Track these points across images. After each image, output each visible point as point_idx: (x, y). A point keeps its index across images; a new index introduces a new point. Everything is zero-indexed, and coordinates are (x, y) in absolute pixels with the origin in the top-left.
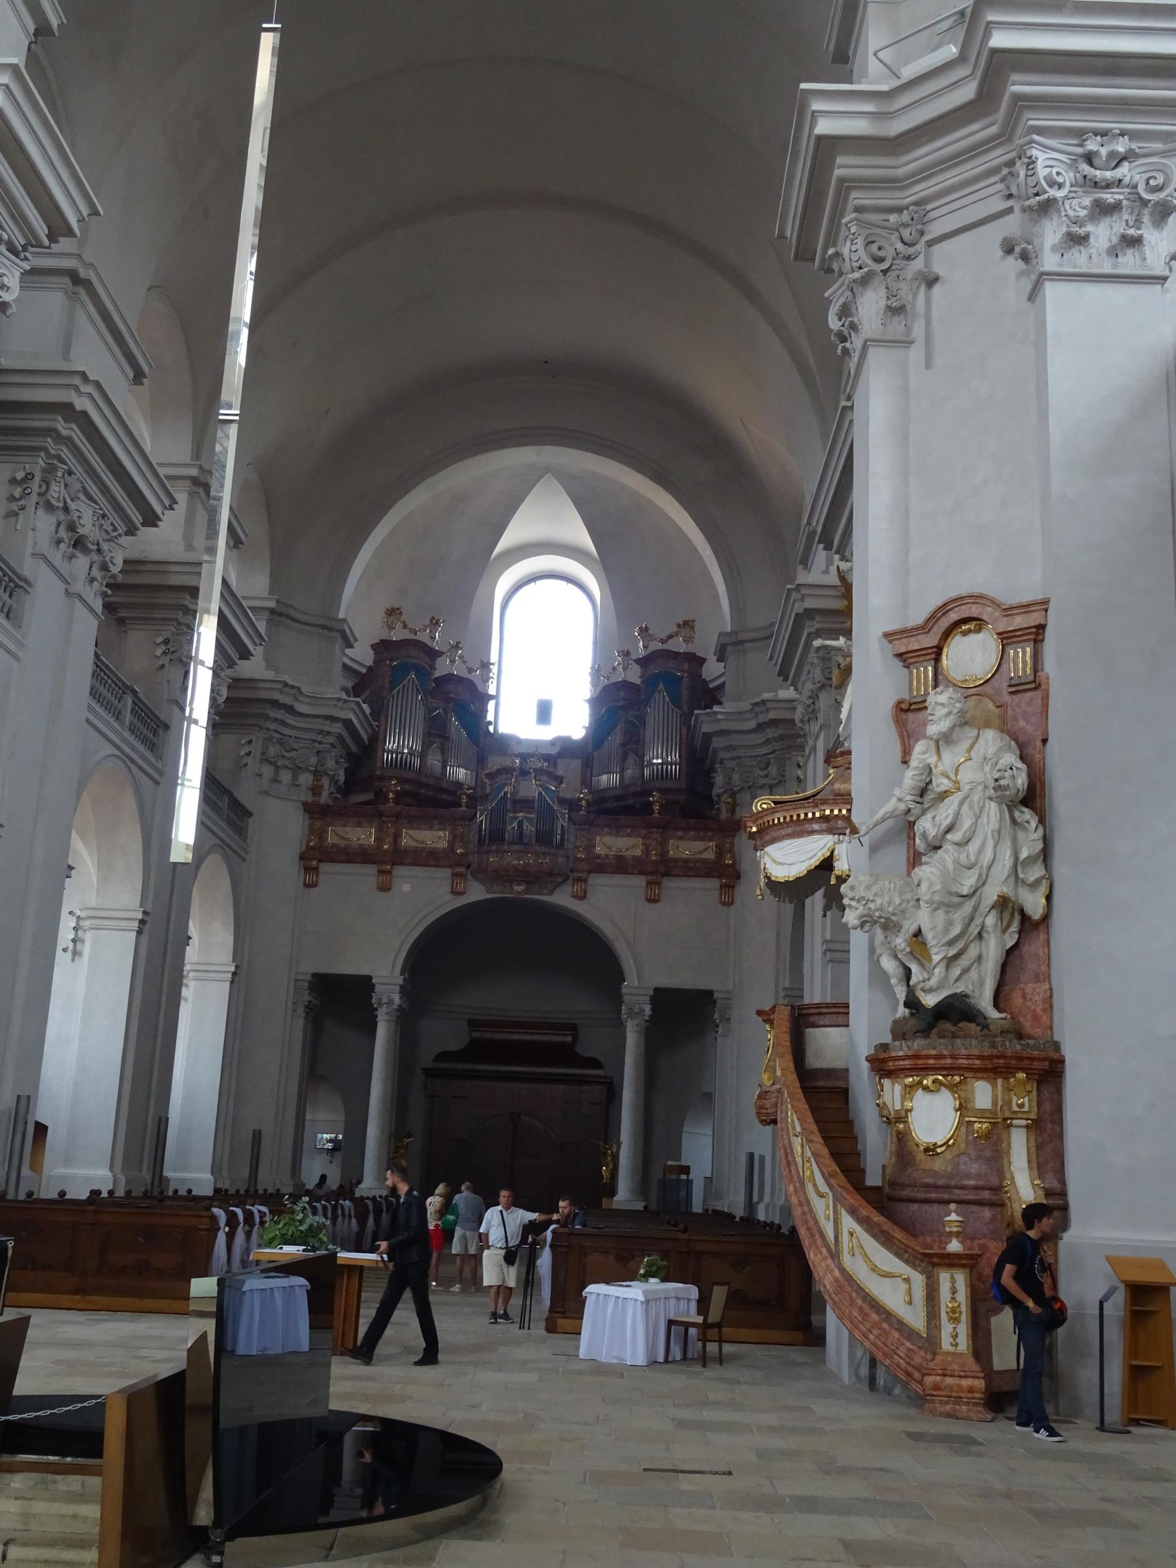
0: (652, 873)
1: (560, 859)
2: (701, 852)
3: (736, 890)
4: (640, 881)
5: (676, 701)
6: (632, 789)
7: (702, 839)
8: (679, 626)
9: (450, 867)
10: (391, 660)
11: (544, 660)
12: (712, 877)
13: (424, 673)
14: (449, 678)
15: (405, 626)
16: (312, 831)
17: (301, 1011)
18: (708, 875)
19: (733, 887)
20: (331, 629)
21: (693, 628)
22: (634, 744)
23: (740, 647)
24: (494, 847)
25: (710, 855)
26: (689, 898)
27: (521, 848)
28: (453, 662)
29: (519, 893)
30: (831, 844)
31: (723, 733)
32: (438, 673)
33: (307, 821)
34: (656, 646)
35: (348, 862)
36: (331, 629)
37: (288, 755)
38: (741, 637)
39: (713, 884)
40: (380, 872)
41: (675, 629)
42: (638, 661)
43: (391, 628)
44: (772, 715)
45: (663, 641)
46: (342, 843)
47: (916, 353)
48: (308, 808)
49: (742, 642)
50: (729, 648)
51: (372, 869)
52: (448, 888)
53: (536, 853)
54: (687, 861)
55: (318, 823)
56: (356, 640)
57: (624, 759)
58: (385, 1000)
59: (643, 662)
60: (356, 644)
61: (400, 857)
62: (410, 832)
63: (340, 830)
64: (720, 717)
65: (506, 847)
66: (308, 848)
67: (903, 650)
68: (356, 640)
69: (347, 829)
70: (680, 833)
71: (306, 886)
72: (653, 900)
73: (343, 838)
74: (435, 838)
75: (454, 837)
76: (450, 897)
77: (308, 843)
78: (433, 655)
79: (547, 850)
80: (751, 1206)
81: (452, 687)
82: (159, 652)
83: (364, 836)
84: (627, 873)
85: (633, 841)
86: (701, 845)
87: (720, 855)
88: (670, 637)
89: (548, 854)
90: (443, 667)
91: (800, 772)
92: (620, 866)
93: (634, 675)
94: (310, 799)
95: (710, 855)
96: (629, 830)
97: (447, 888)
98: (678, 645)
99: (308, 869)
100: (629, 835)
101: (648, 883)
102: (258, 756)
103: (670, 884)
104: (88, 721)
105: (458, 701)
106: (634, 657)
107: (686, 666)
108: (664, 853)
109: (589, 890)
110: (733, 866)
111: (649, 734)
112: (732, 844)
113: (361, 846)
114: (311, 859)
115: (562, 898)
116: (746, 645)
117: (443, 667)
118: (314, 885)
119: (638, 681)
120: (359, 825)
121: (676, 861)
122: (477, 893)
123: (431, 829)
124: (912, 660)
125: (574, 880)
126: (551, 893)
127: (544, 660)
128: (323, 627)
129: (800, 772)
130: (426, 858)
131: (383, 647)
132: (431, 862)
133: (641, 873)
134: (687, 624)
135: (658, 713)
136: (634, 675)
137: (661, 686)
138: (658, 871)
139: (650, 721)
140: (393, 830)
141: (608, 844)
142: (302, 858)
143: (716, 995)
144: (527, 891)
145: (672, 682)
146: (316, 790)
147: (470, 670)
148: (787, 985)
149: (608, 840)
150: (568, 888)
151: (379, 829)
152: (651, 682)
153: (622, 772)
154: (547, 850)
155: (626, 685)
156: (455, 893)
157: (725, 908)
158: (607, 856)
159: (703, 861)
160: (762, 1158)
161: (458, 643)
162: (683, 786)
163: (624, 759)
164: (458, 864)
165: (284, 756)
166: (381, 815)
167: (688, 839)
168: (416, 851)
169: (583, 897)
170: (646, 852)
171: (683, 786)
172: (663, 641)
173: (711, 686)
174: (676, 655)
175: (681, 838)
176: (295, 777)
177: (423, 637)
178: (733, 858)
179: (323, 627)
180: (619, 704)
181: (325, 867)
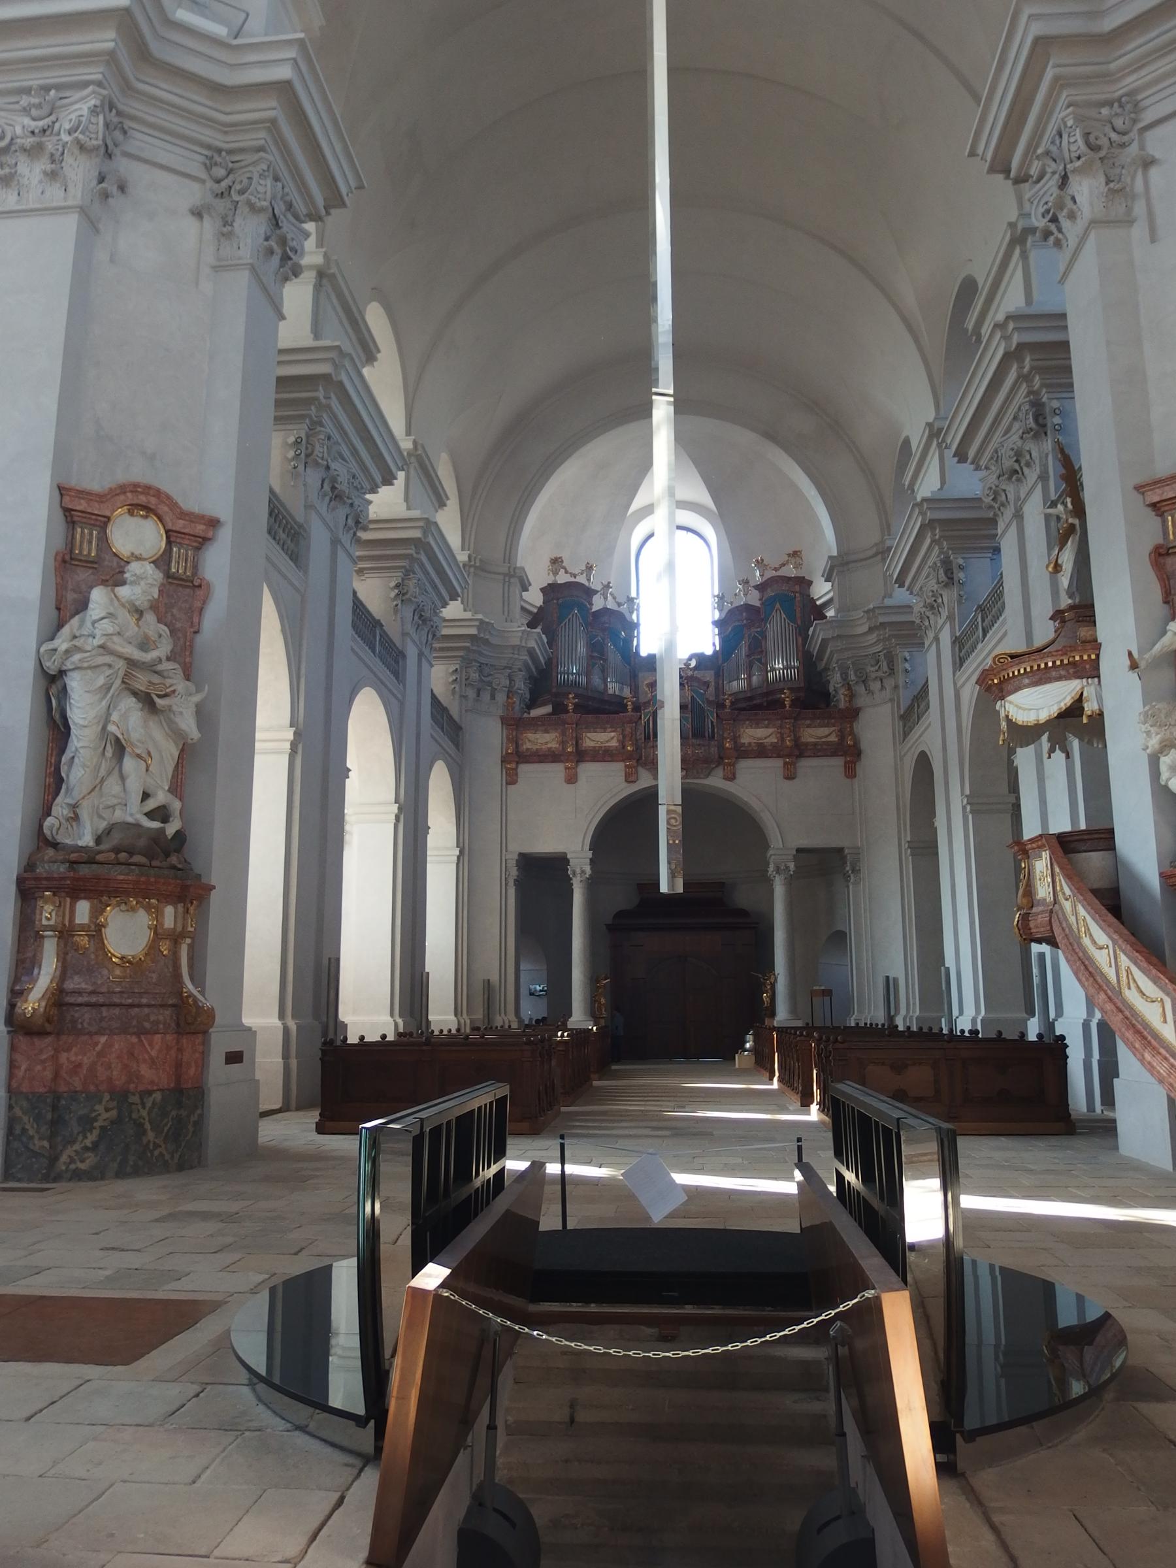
0: (788, 756)
4: (777, 764)
5: (791, 617)
6: (759, 691)
7: (827, 726)
8: (789, 555)
11: (676, 596)
13: (584, 608)
14: (605, 611)
15: (566, 572)
17: (511, 883)
18: (834, 754)
22: (758, 653)
25: (833, 738)
26: (818, 774)
28: (606, 598)
30: (1079, 687)
32: (594, 609)
34: (770, 574)
39: (838, 762)
40: (567, 768)
42: (757, 587)
43: (556, 573)
44: (882, 619)
45: (776, 569)
47: (1138, 232)
48: (504, 721)
49: (847, 563)
54: (815, 744)
57: (750, 666)
58: (578, 871)
59: (761, 588)
61: (581, 755)
63: (530, 736)
66: (507, 753)
67: (1156, 499)
69: (537, 736)
70: (808, 722)
75: (624, 737)
76: (626, 784)
78: (589, 593)
80: (891, 1018)
81: (605, 619)
82: (393, 594)
83: (546, 740)
85: (770, 731)
87: (842, 738)
88: (783, 565)
90: (598, 603)
91: (907, 666)
92: (761, 752)
95: (833, 738)
98: (790, 571)
100: (767, 727)
101: (785, 764)
102: (464, 682)
104: (352, 649)
105: (611, 628)
106: (752, 583)
107: (797, 588)
108: (796, 740)
111: (770, 645)
112: (852, 727)
116: (851, 566)
117: (598, 603)
118: (514, 782)
119: (758, 604)
120: (547, 731)
121: (807, 744)
124: (1167, 508)
126: (707, 776)
127: (676, 596)
129: (907, 666)
130: (603, 755)
131: (550, 591)
133: (779, 756)
134: (796, 554)
135: (777, 628)
136: (754, 599)
137: (778, 606)
138: (793, 754)
139: (770, 635)
141: (752, 734)
143: (846, 851)
145: (786, 602)
146: (509, 706)
147: (619, 605)
148: (909, 839)
150: (719, 772)
151: (563, 734)
152: (768, 603)
153: (750, 677)
155: (747, 607)
157: (849, 780)
158: (750, 744)
159: (828, 743)
160: (896, 980)
162: (802, 685)
163: (750, 666)
166: (564, 723)
169: (731, 777)
170: (782, 739)
171: (802, 685)
172: (776, 569)
173: (818, 603)
175: (809, 726)
177: (582, 579)
180: (741, 625)
181: (523, 768)
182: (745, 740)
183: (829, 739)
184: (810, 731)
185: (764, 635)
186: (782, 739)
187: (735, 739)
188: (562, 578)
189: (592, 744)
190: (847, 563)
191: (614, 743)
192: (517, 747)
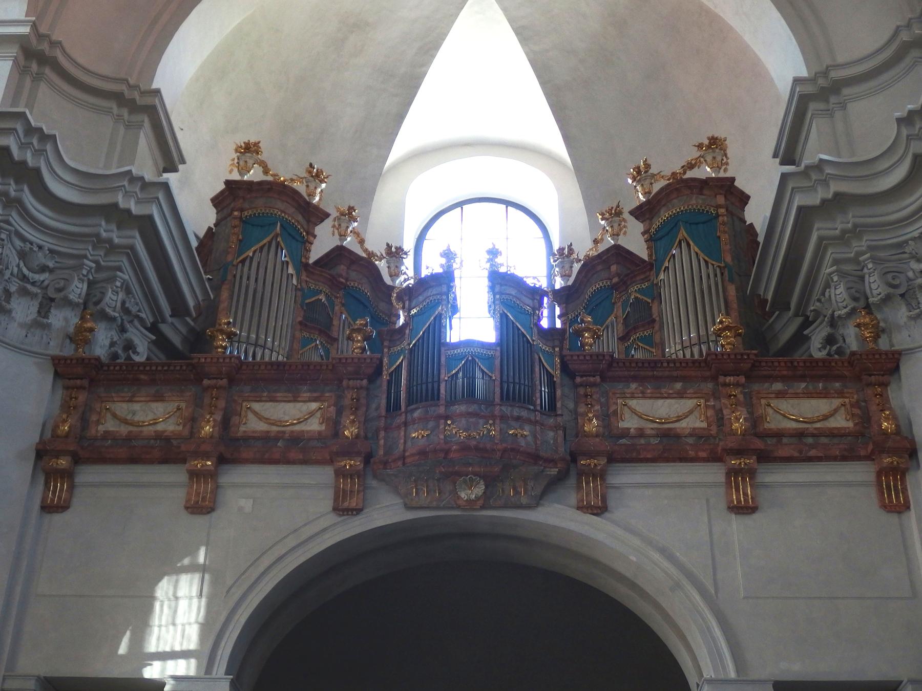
0: (739, 452)
1: (551, 434)
2: (826, 418)
3: (909, 479)
4: (714, 474)
8: (700, 146)
9: (331, 462)
10: (242, 210)
12: (859, 458)
15: (266, 172)
16: (66, 407)
18: (848, 456)
19: (903, 474)
20: (133, 107)
21: (724, 150)
23: (833, 99)
24: (416, 414)
27: (473, 408)
29: (470, 504)
31: (840, 202)
33: (60, 393)
35: (133, 460)
36: (133, 107)
37: (37, 277)
38: (835, 74)
39: (861, 473)
41: (696, 153)
43: (243, 170)
46: (124, 430)
48: (63, 370)
49: (836, 87)
50: (813, 106)
51: (175, 475)
52: (329, 504)
53: (503, 418)
54: (800, 435)
55: (82, 397)
56: (183, 162)
60: (181, 167)
61: (232, 450)
62: (256, 406)
63: (121, 408)
64: (829, 170)
65: (442, 410)
68: (183, 162)
69: (136, 407)
70: (778, 386)
71: (48, 508)
72: (744, 509)
73: (125, 422)
74: (299, 414)
75: (339, 412)
76: (333, 518)
77: (56, 427)
79: (524, 414)
81: (342, 269)
84: (684, 459)
85: (689, 404)
86: (822, 406)
87: (865, 419)
89: (529, 421)
92: (669, 448)
93: (635, 241)
94: (68, 351)
95: (841, 422)
96: (678, 386)
97: (325, 501)
98: (706, 171)
99: (52, 475)
100: (681, 395)
103: (772, 475)
107: (721, 200)
108: (755, 421)
109: (613, 498)
110: (898, 432)
113: (159, 436)
114: (58, 454)
115: (560, 517)
116: (846, 91)
118: (62, 507)
120: (158, 398)
121: (779, 435)
122: (385, 511)
123: (295, 400)
125: (580, 475)
126: (536, 502)
128: (118, 97)
131: (231, 196)
132: (292, 455)
133: (715, 458)
137: (683, 233)
138: (746, 458)
139: (668, 293)
140: (222, 404)
142: (41, 453)
144: (486, 502)
145: (700, 225)
149: (640, 405)
154: (524, 414)
156: (344, 508)
157: (893, 518)
158: (641, 433)
159: (833, 434)
161: (351, 209)
164: (347, 452)
165: (24, 278)
167: (796, 396)
168: (266, 439)
169: (600, 510)
174: (704, 184)
175: (780, 395)
176: (44, 311)
178: (894, 418)
179: (118, 97)
182: (629, 423)
183: (833, 423)
184: (785, 405)
185: (655, 293)
186: (720, 420)
187: (607, 417)
188: (254, 174)
189: (262, 427)
190: (836, 87)
191: (315, 426)
192: (84, 422)
